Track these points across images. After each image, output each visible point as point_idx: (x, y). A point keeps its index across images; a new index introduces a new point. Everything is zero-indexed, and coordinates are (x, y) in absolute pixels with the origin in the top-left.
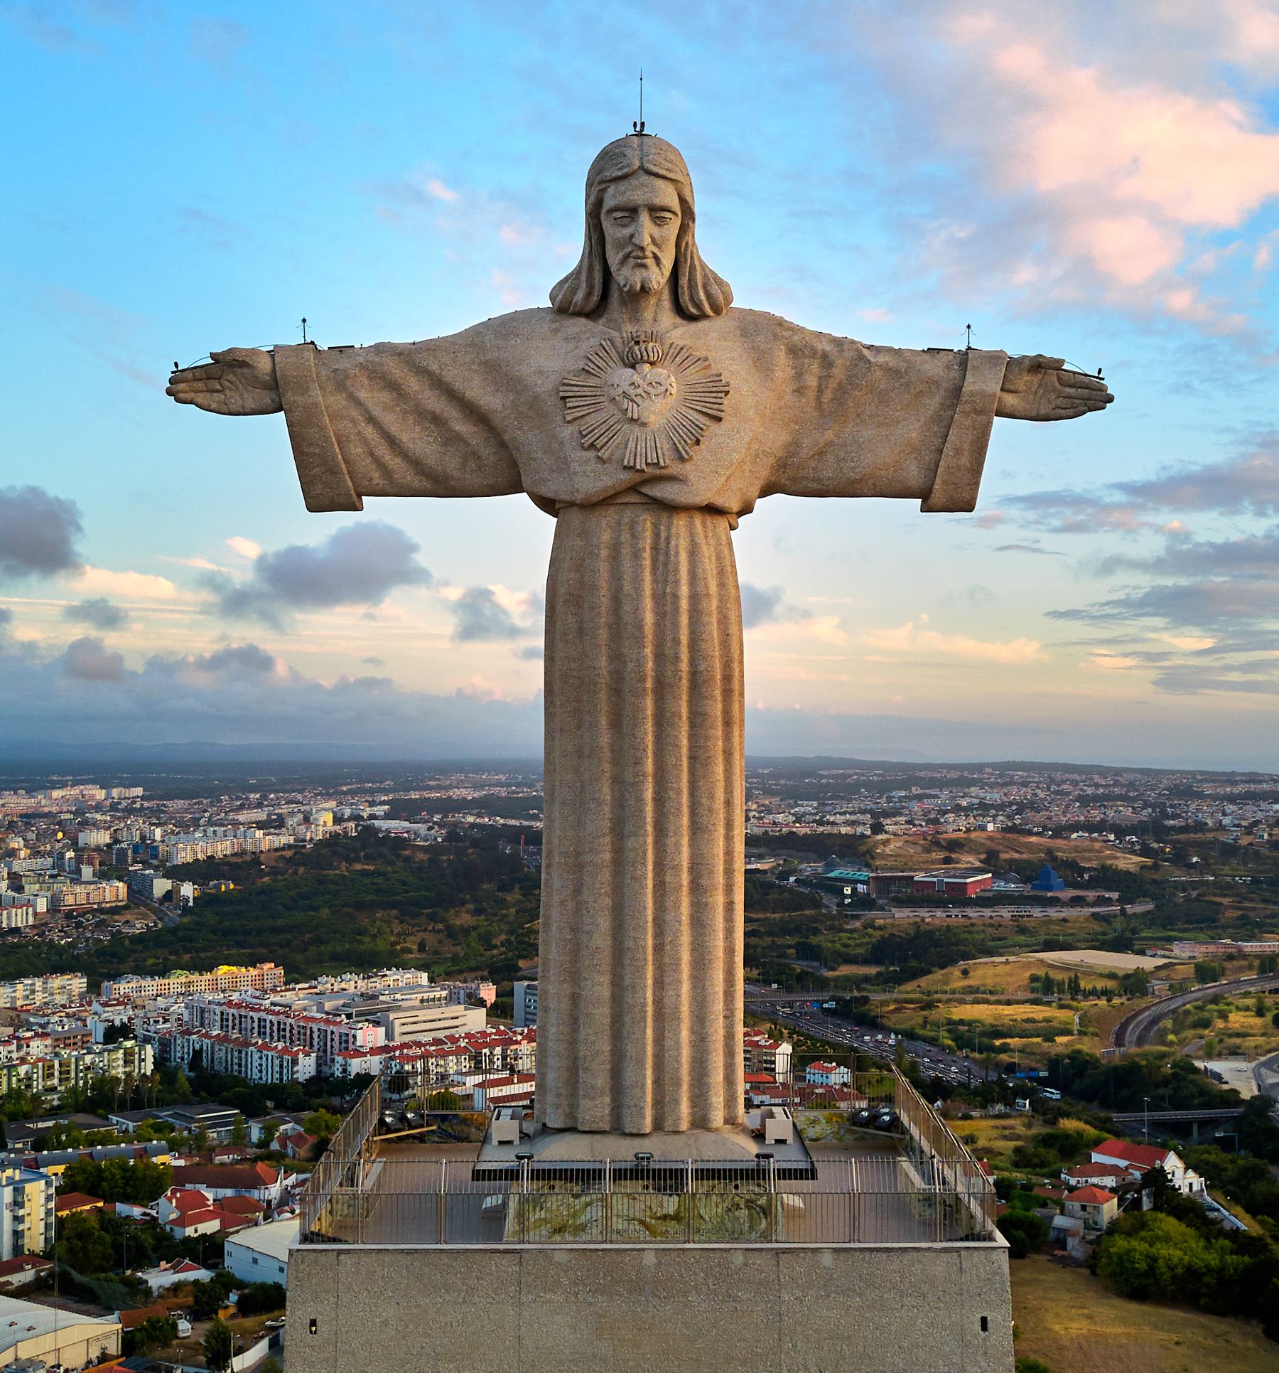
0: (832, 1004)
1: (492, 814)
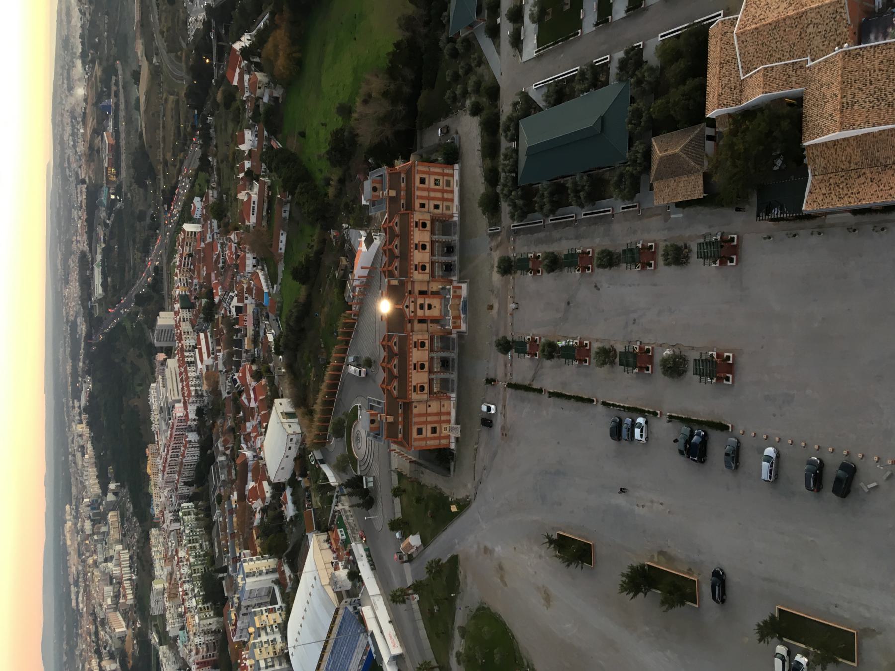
0: (166, 206)
1: (78, 354)
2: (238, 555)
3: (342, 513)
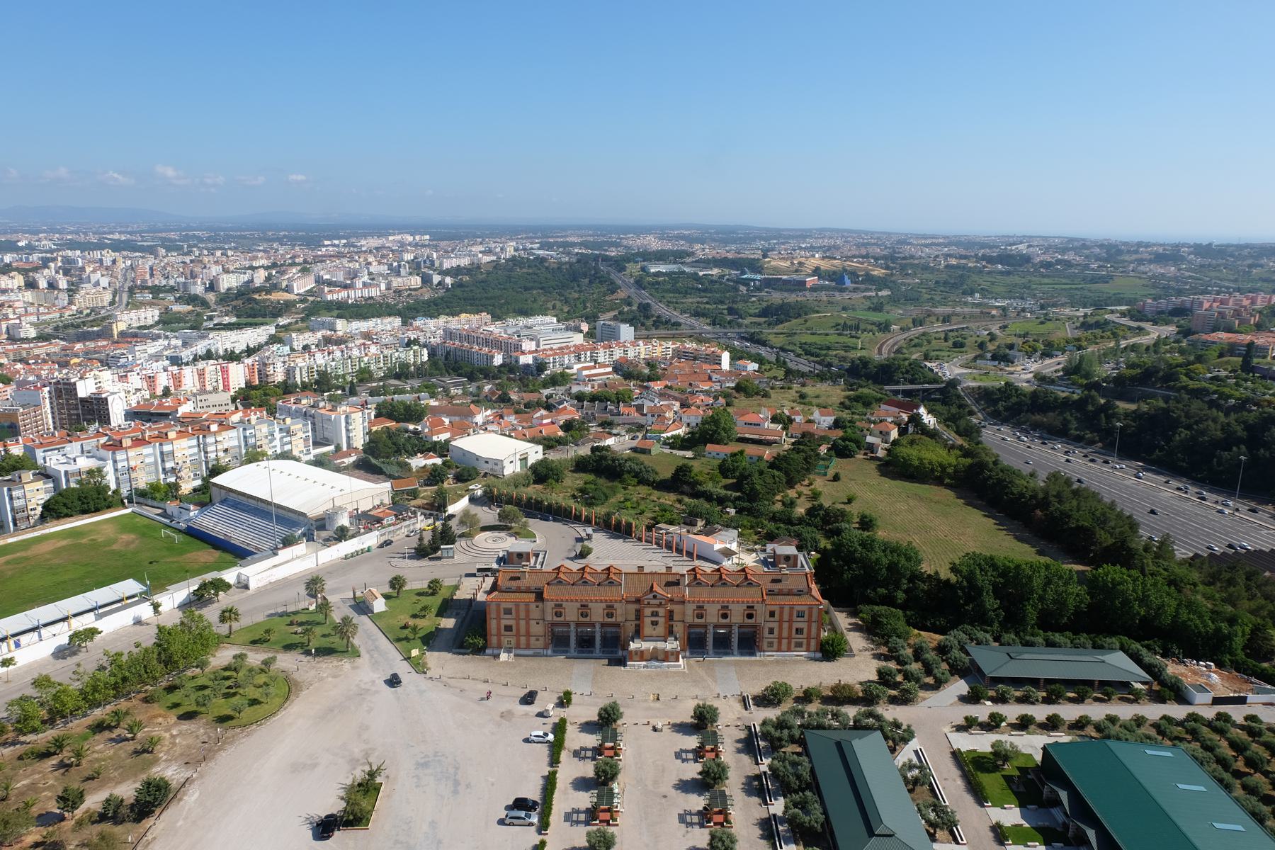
3: (413, 521)
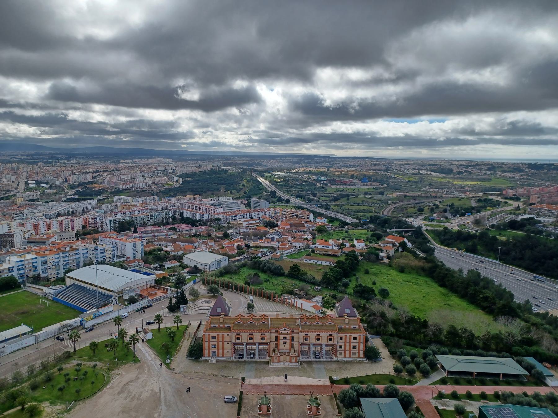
0: (320, 205)
2: (144, 239)
